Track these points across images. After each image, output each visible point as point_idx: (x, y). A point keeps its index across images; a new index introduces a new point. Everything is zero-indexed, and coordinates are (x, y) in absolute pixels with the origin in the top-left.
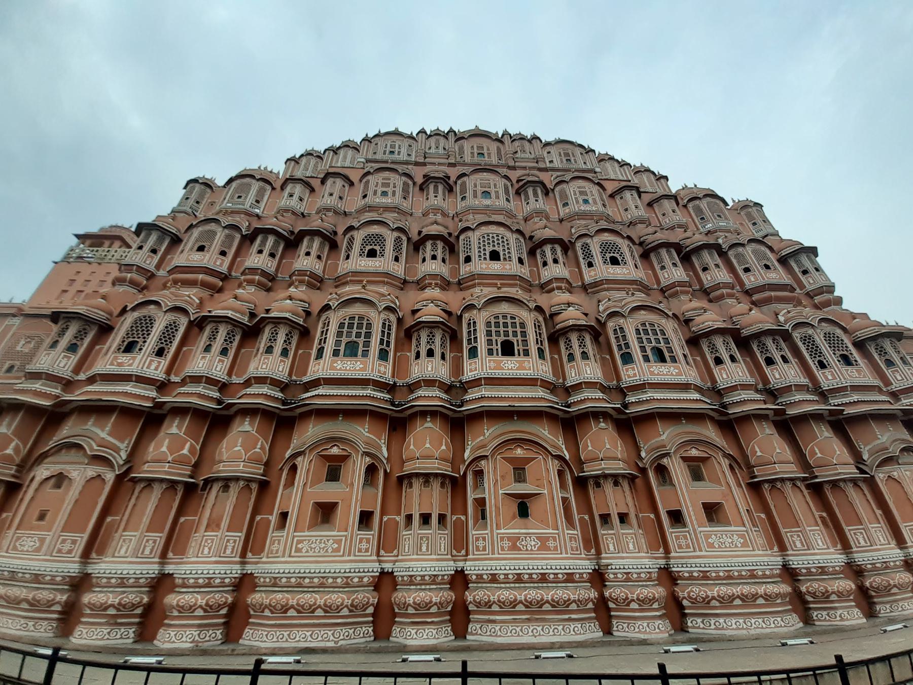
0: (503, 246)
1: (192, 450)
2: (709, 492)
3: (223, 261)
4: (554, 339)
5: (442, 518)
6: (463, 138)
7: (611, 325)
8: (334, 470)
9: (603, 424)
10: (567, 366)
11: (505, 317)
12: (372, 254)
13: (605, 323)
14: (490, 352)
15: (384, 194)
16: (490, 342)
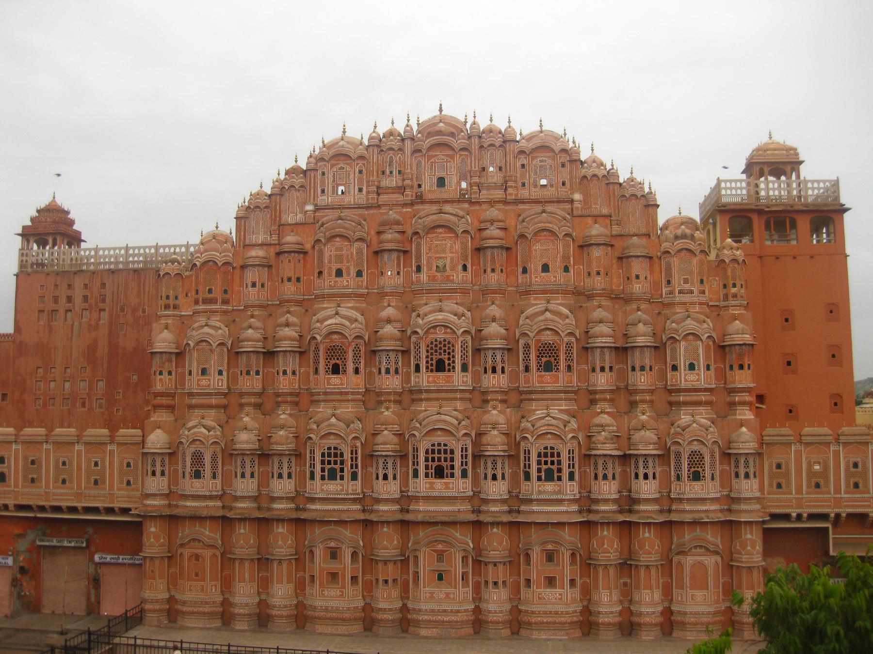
0: (449, 354)
1: (254, 539)
2: (551, 570)
3: (222, 380)
4: (477, 457)
5: (395, 581)
6: (420, 151)
7: (522, 444)
8: (334, 554)
9: (495, 530)
10: (483, 482)
11: (439, 445)
12: (336, 370)
13: (519, 443)
14: (427, 475)
15: (339, 273)
16: (427, 467)
